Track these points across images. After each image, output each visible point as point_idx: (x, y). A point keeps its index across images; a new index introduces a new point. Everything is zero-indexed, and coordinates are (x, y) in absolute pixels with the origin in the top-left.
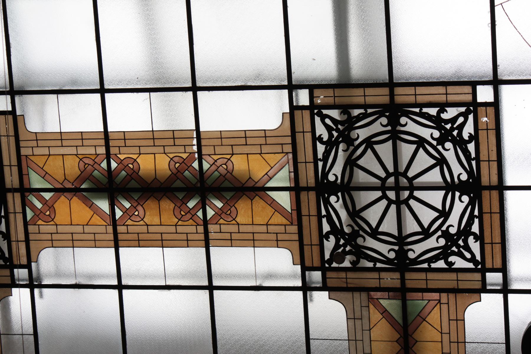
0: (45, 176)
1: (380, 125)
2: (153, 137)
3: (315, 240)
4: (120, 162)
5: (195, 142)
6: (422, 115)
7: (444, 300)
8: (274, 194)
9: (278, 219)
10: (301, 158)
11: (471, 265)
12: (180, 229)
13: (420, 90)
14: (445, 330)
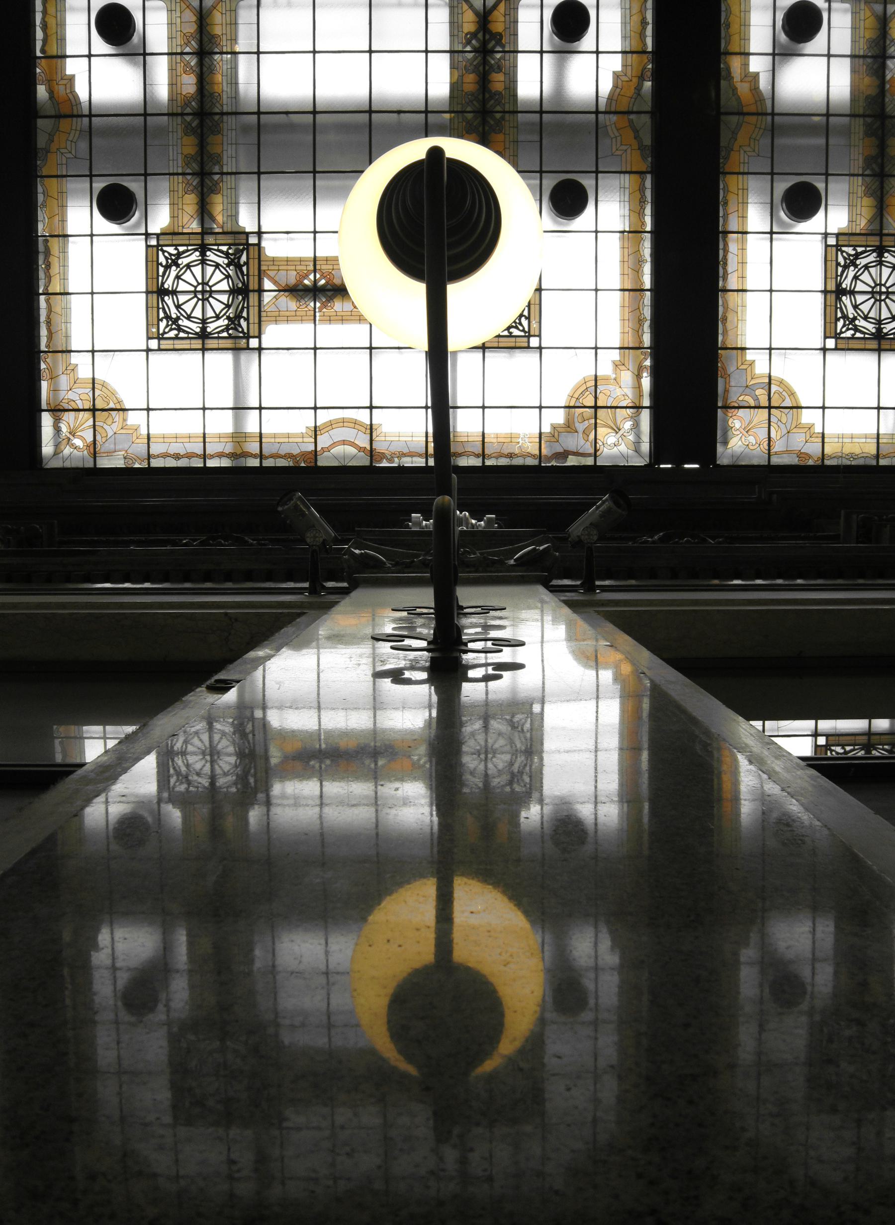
1: (211, 327)
3: (251, 261)
5: (317, 318)
6: (188, 333)
7: (180, 228)
8: (275, 288)
9: (272, 274)
10: (256, 309)
11: (165, 248)
12: (331, 267)
13: (171, 347)
14: (180, 211)
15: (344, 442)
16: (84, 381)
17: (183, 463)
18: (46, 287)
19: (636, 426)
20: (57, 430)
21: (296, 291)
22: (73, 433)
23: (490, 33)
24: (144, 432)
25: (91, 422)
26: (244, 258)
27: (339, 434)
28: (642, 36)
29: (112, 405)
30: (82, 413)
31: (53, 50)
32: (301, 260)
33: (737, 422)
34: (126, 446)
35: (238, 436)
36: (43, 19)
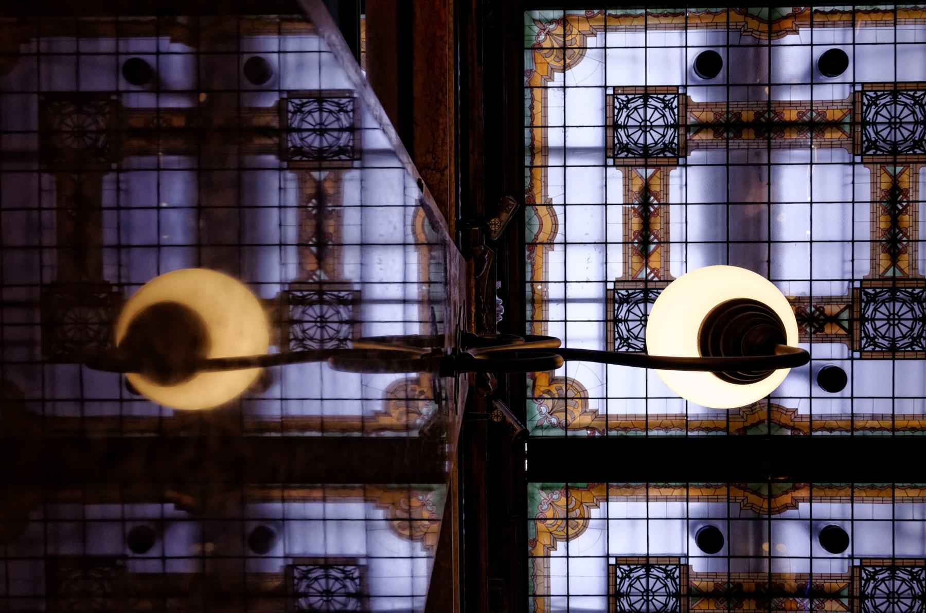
0: (640, 270)
2: (626, 223)
4: (635, 238)
9: (658, 174)
15: (541, 225)
16: (585, 41)
17: (527, 112)
18: (651, 14)
19: (553, 426)
20: (551, 22)
21: (646, 190)
22: (548, 34)
23: (825, 323)
24: (550, 84)
25: (556, 46)
26: (669, 155)
27: (547, 222)
28: (822, 428)
29: (568, 61)
30: (562, 39)
31: (817, 19)
32: (667, 194)
33: (558, 497)
34: (540, 71)
35: (546, 150)
36: (839, 11)
